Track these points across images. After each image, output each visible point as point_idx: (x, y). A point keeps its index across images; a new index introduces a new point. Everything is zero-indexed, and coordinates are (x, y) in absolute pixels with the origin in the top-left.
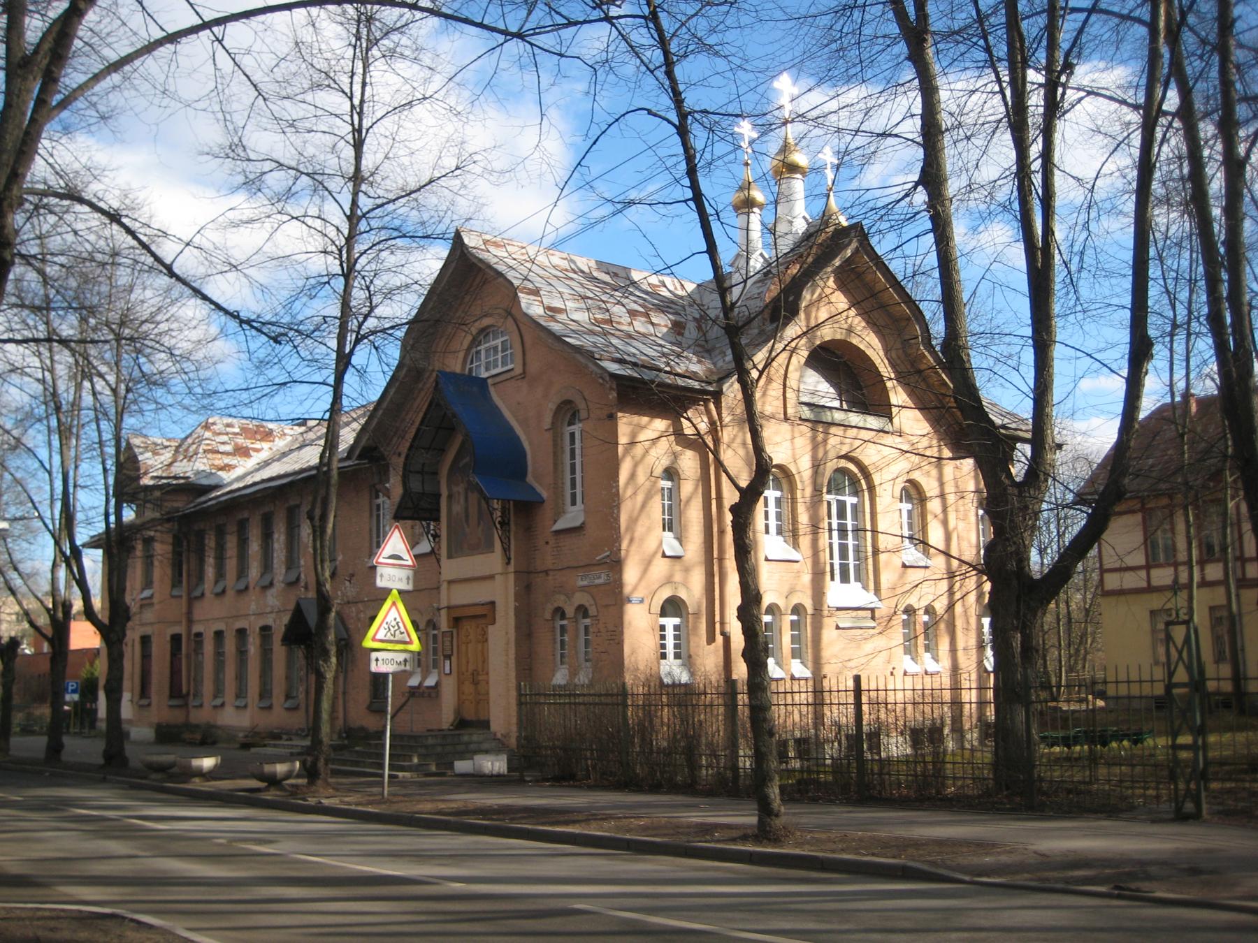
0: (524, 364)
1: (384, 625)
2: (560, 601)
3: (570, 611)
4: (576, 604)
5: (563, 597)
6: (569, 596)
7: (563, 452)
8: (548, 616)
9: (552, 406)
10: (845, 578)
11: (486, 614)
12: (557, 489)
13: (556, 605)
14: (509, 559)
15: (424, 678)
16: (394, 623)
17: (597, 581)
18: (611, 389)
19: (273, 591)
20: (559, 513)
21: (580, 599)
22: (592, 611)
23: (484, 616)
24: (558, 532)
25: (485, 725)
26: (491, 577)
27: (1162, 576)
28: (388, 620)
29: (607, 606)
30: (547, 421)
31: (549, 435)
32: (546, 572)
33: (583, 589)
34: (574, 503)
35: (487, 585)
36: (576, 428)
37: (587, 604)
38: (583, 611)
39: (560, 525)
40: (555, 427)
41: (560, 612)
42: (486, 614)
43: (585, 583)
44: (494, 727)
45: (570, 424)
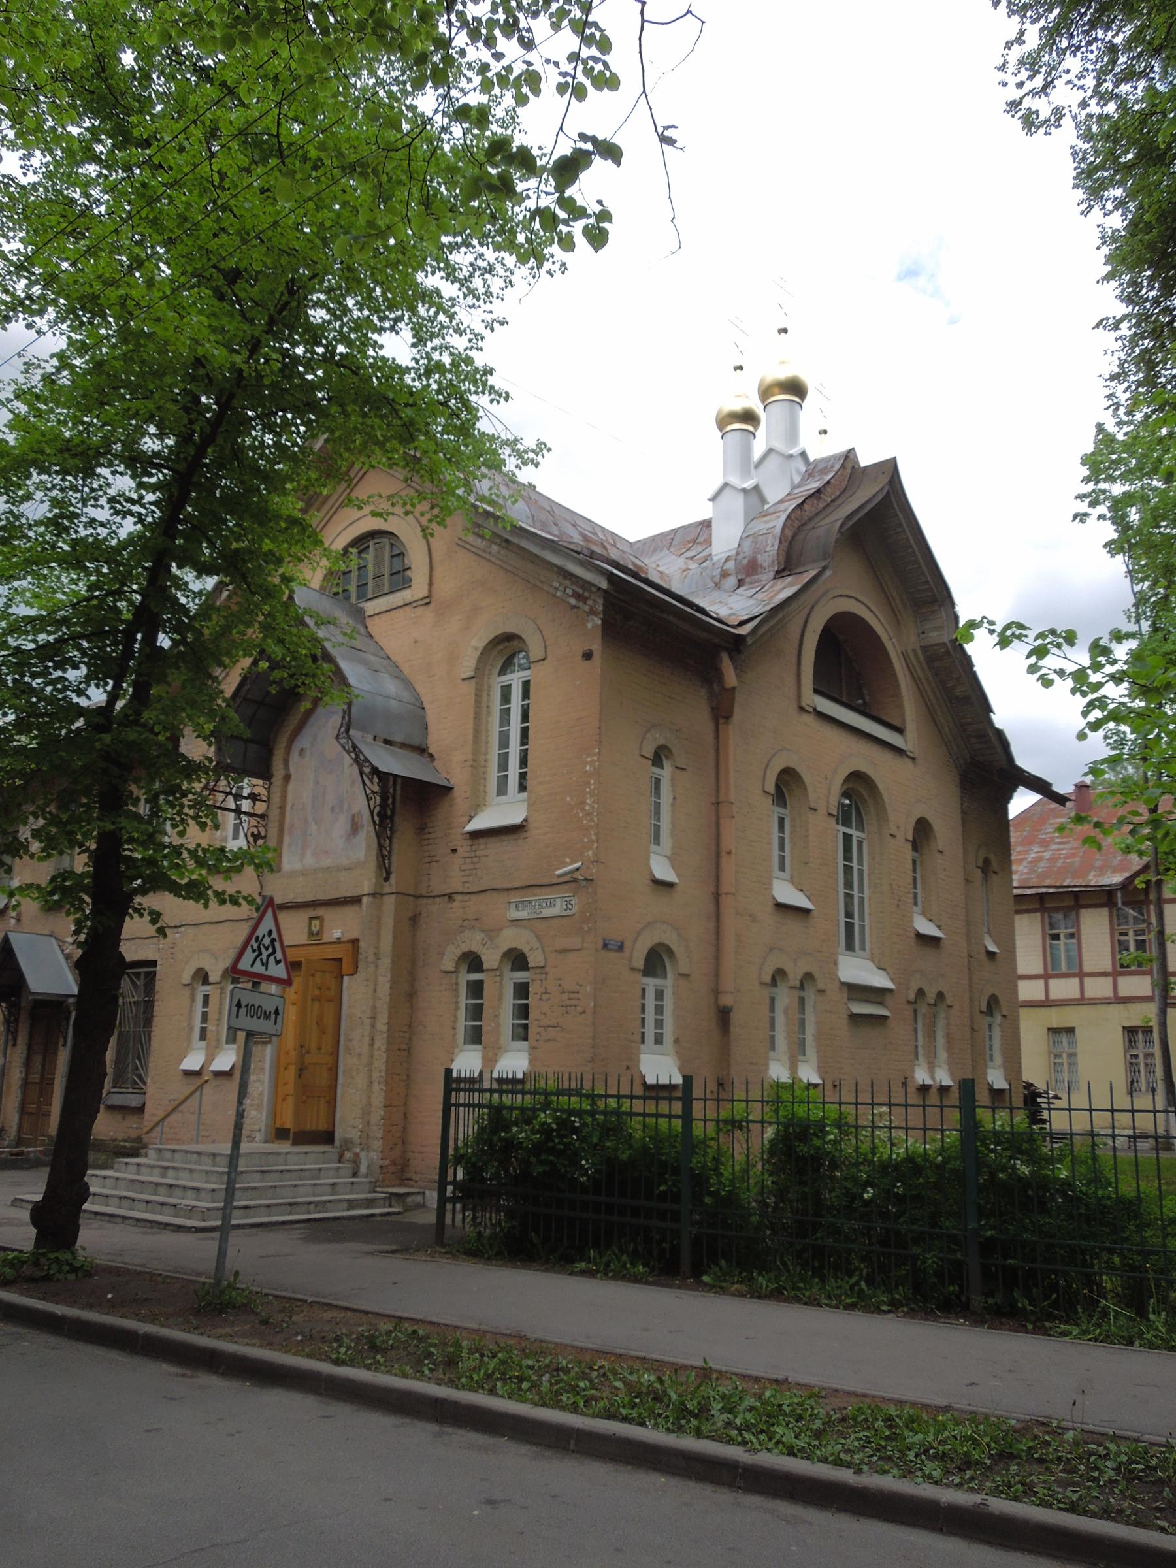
0: (430, 584)
1: (253, 942)
2: (473, 941)
3: (491, 958)
4: (505, 948)
5: (479, 936)
6: (492, 933)
7: (489, 714)
8: (448, 964)
9: (479, 640)
10: (850, 946)
12: (477, 766)
14: (389, 873)
15: (210, 1058)
16: (267, 941)
17: (547, 912)
18: (592, 612)
20: (476, 807)
21: (510, 939)
22: (534, 959)
24: (476, 835)
26: (356, 900)
27: (1064, 988)
28: (261, 932)
29: (563, 951)
30: (468, 665)
31: (470, 687)
32: (450, 897)
34: (502, 789)
35: (349, 912)
36: (515, 679)
37: (526, 950)
38: (518, 960)
39: (476, 824)
40: (478, 676)
41: (473, 962)
43: (523, 914)
45: (503, 672)
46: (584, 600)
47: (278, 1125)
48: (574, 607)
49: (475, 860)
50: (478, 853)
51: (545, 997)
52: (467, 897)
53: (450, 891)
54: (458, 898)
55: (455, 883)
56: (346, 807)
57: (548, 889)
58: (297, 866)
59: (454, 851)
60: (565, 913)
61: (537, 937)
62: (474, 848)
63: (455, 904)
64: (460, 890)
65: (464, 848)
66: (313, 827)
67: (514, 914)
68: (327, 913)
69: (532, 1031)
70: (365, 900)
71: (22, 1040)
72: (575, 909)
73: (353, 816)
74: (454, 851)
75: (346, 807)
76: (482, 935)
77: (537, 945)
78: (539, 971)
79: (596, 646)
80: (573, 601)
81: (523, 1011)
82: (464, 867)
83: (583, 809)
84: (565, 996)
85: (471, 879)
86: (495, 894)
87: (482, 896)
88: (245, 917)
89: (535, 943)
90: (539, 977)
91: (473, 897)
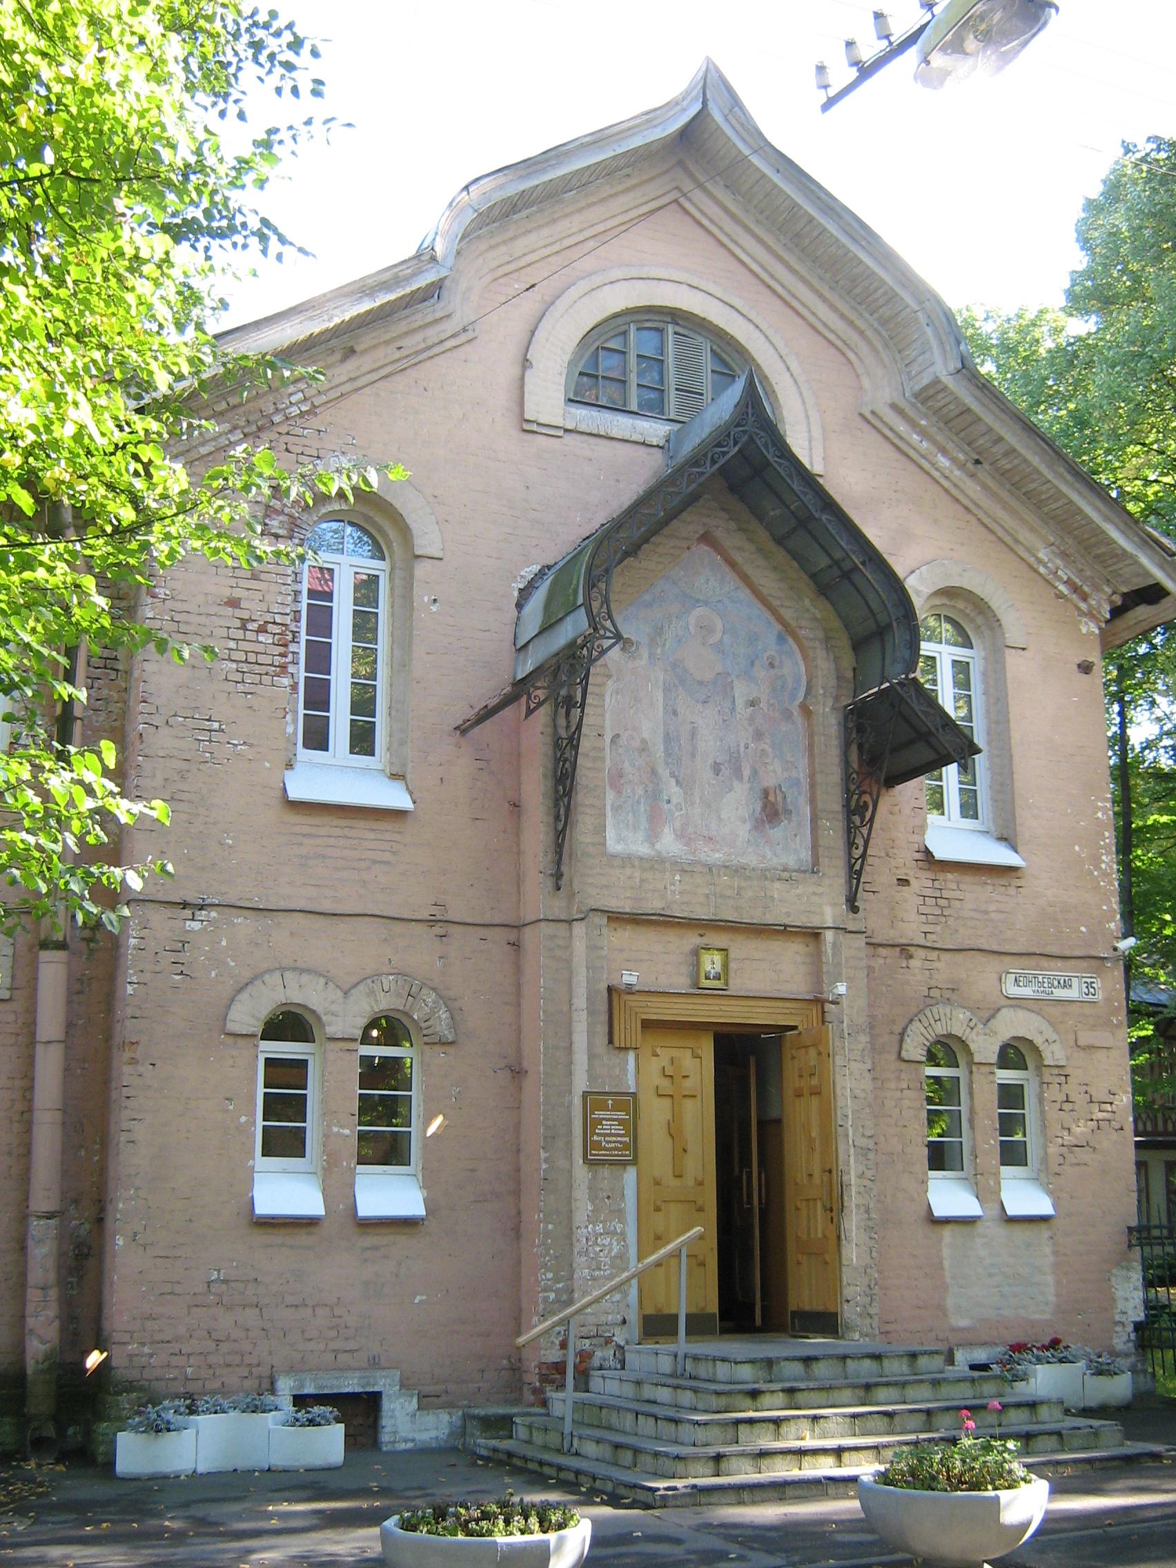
2: (957, 1022)
3: (985, 1047)
5: (962, 1015)
13: (940, 1029)
17: (1060, 993)
18: (1091, 615)
21: (1011, 1025)
22: (1054, 1054)
26: (814, 934)
32: (905, 950)
33: (1018, 1003)
37: (1038, 1041)
43: (1027, 992)
46: (1084, 598)
47: (650, 1310)
48: (1060, 596)
49: (941, 902)
50: (945, 894)
51: (1067, 1106)
52: (934, 955)
53: (903, 941)
54: (921, 953)
55: (911, 928)
56: (747, 772)
57: (1060, 963)
58: (642, 849)
59: (903, 882)
60: (1086, 998)
61: (1051, 1024)
62: (937, 884)
63: (914, 963)
64: (922, 942)
65: (921, 881)
66: (673, 790)
67: (1012, 990)
68: (741, 948)
69: (1033, 1153)
70: (829, 936)
72: (1100, 996)
73: (766, 793)
74: (903, 882)
75: (747, 772)
76: (968, 1014)
77: (1055, 1037)
78: (1056, 1071)
79: (1095, 657)
80: (1062, 588)
81: (1008, 1124)
82: (923, 909)
83: (1098, 868)
84: (1095, 1107)
85: (938, 928)
86: (980, 957)
87: (959, 957)
88: (425, 915)
90: (1058, 1079)
91: (946, 957)
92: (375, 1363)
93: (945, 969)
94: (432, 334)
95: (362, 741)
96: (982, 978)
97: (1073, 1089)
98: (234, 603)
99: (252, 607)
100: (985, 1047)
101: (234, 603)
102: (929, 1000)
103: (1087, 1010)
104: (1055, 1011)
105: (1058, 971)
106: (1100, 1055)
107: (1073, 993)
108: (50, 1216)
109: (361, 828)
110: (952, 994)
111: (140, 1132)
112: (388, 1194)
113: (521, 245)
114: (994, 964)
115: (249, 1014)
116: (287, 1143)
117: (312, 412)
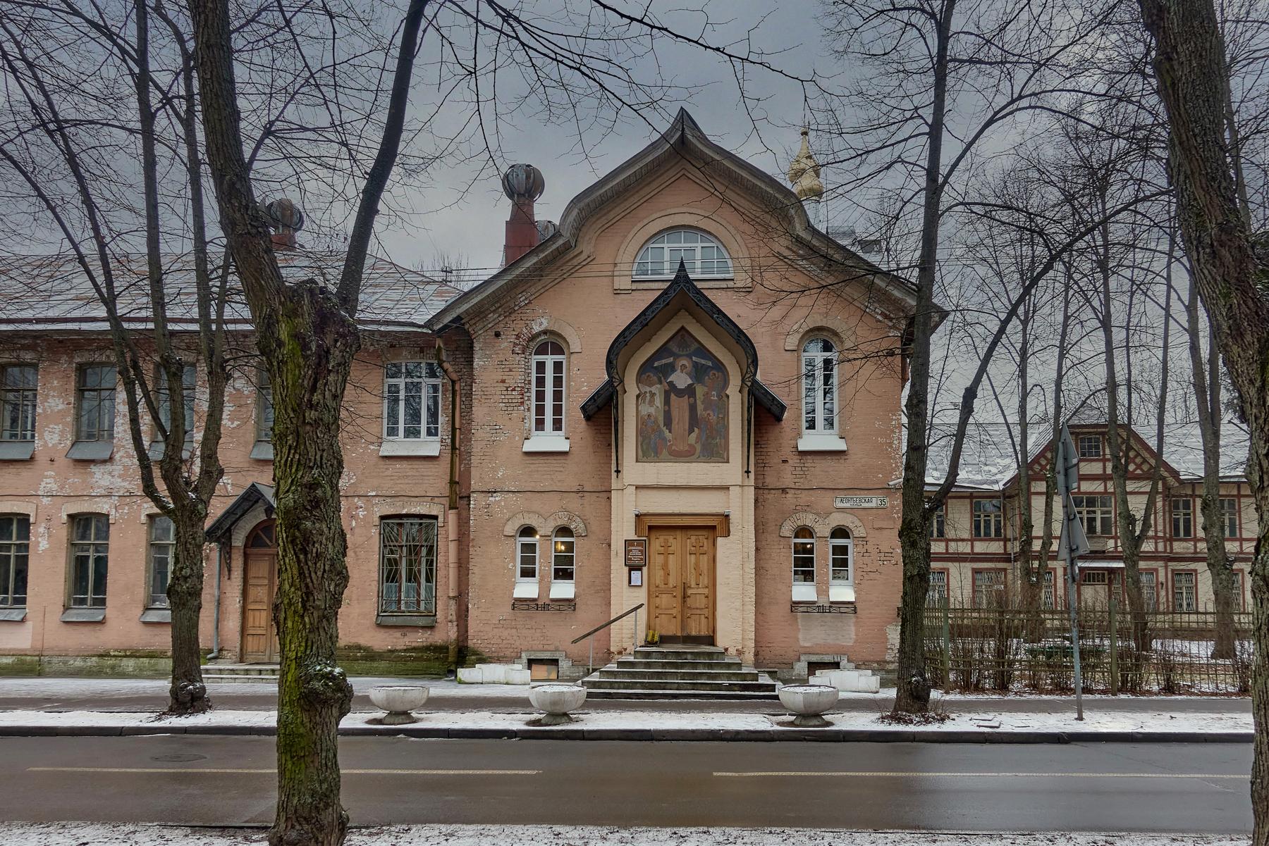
2: (808, 520)
3: (823, 529)
5: (811, 516)
11: (716, 526)
13: (799, 523)
17: (865, 505)
18: (894, 327)
19: (117, 468)
21: (837, 520)
22: (858, 531)
23: (714, 528)
25: (711, 640)
35: (719, 495)
37: (851, 526)
38: (840, 532)
42: (716, 526)
43: (848, 505)
44: (722, 641)
46: (891, 319)
55: (788, 480)
59: (785, 461)
65: (794, 460)
67: (840, 505)
71: (237, 574)
74: (785, 461)
80: (879, 317)
89: (858, 523)
92: (557, 650)
93: (804, 497)
94: (575, 262)
95: (557, 425)
96: (825, 500)
97: (870, 547)
98: (503, 381)
99: (510, 382)
100: (823, 529)
101: (503, 381)
102: (795, 511)
103: (880, 512)
104: (863, 513)
105: (863, 495)
106: (885, 532)
107: (873, 505)
108: (454, 598)
109: (551, 460)
110: (807, 508)
111: (476, 570)
112: (562, 590)
113: (611, 215)
114: (830, 493)
115: (511, 528)
116: (528, 573)
117: (530, 302)
